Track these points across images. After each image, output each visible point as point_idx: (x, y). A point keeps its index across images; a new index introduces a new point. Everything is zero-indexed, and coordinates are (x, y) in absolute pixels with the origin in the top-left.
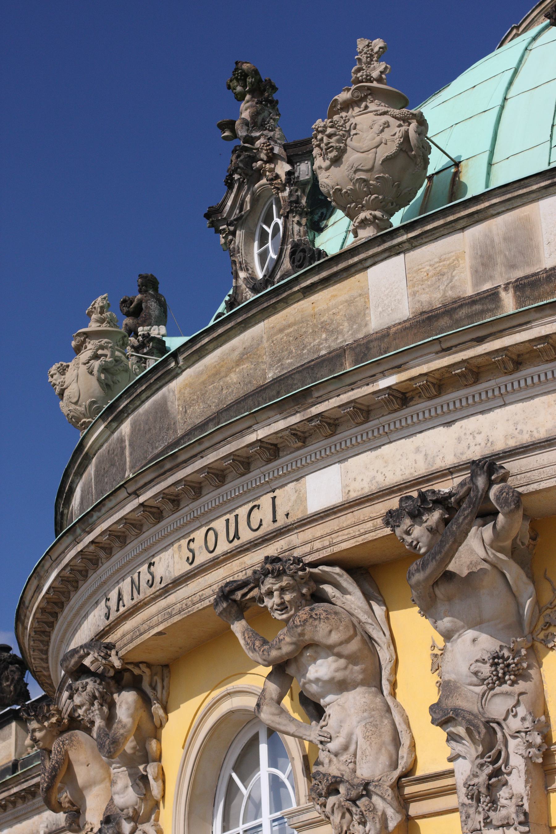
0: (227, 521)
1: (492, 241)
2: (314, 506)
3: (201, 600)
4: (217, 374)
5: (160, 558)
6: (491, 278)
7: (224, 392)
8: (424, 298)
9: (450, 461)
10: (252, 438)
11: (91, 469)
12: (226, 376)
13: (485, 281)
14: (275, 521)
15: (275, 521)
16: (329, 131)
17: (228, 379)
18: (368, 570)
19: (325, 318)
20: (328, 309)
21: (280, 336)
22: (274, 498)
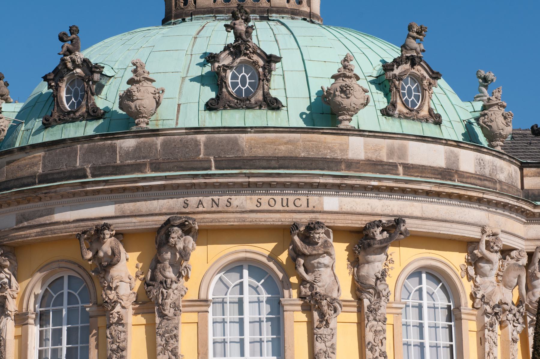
0: (282, 199)
1: (394, 147)
2: (326, 208)
3: (265, 221)
4: (273, 142)
5: (236, 199)
6: (393, 159)
7: (277, 151)
8: (370, 155)
9: (379, 211)
10: (318, 181)
11: (159, 140)
12: (278, 145)
13: (391, 159)
14: (308, 207)
15: (308, 207)
16: (352, 88)
17: (279, 147)
18: (341, 233)
19: (330, 145)
20: (331, 143)
21: (308, 143)
22: (308, 199)
